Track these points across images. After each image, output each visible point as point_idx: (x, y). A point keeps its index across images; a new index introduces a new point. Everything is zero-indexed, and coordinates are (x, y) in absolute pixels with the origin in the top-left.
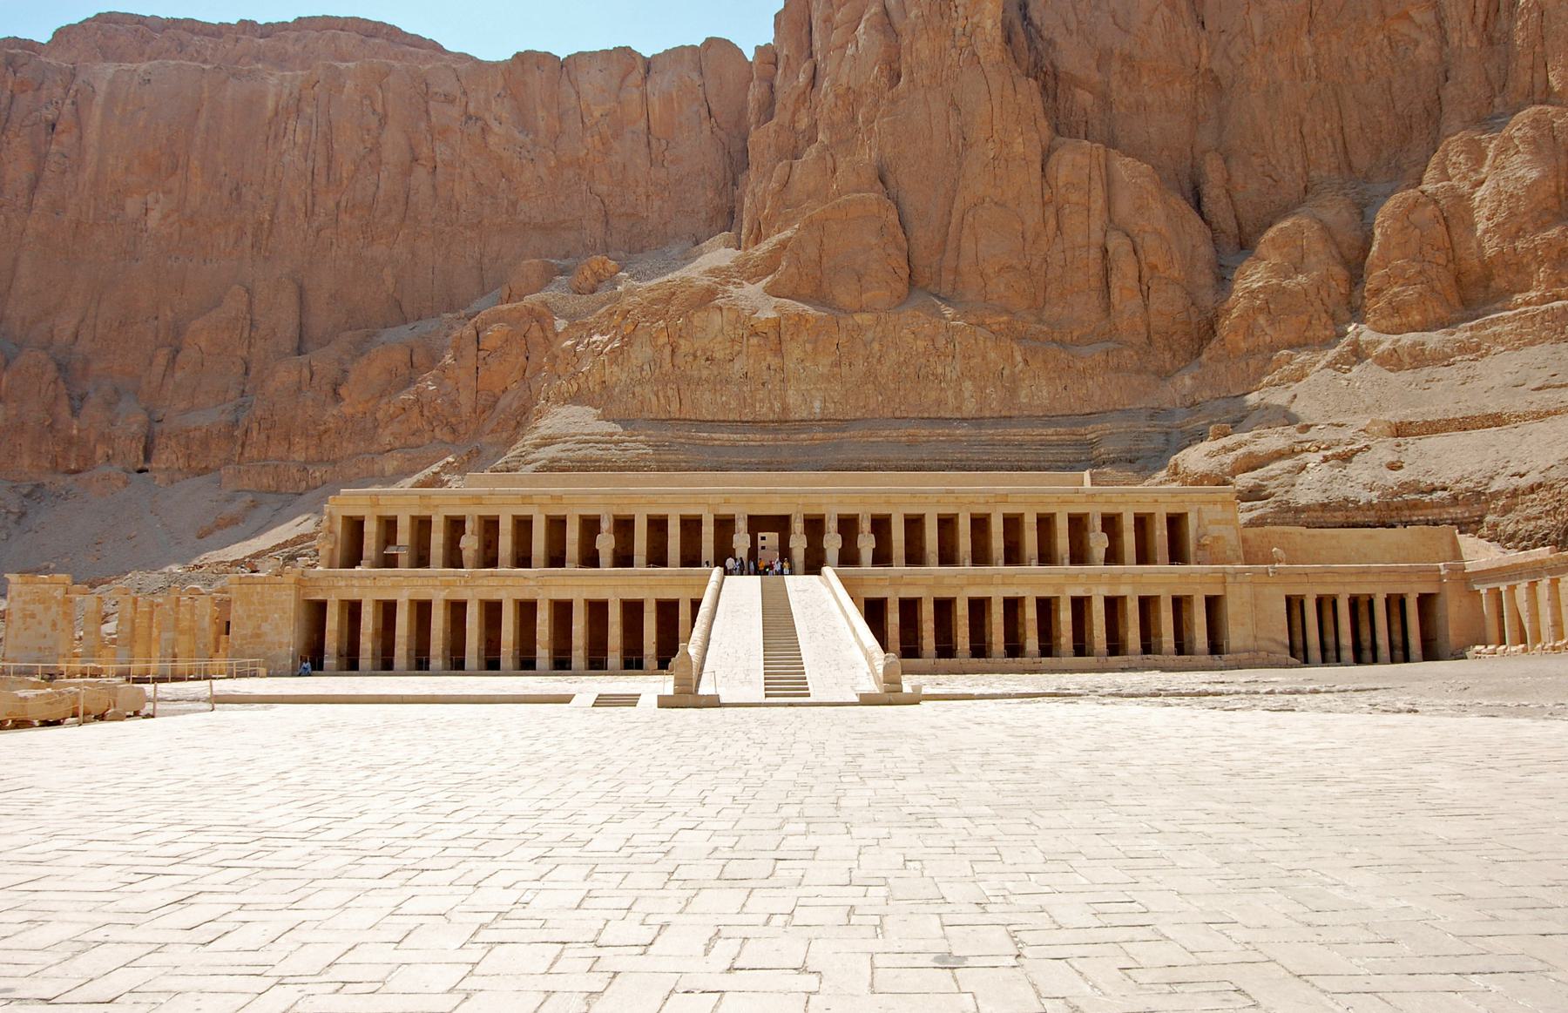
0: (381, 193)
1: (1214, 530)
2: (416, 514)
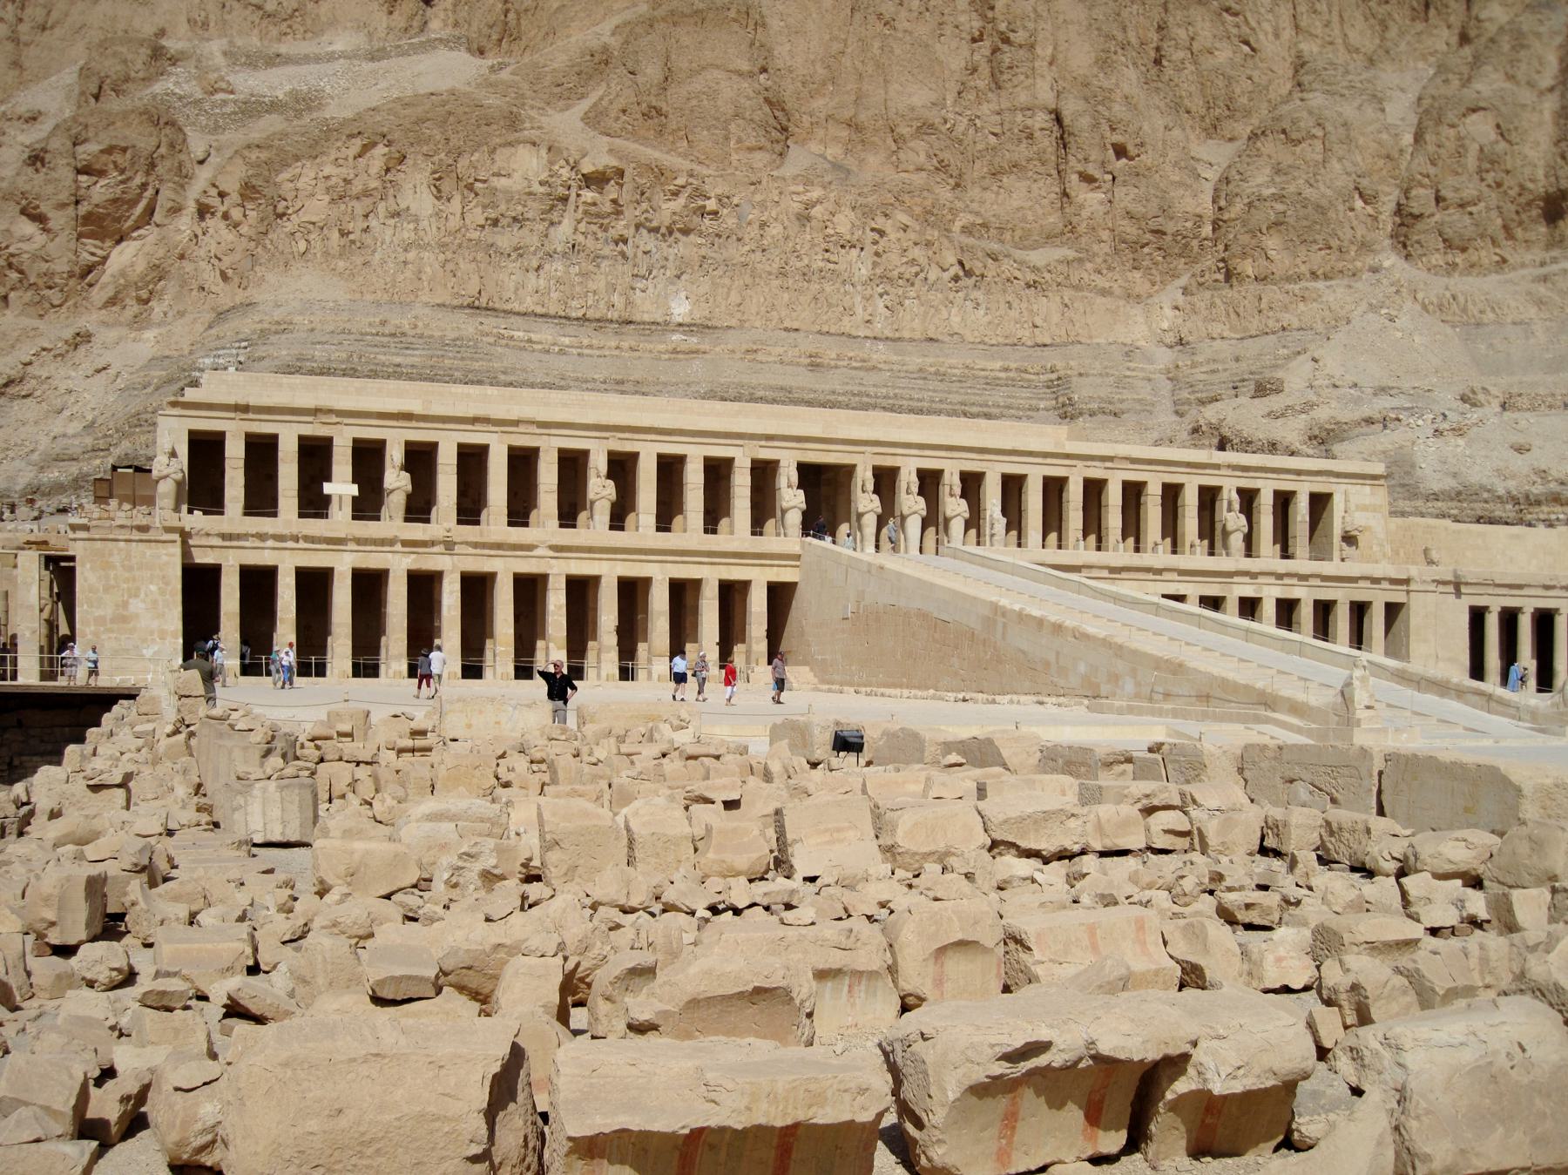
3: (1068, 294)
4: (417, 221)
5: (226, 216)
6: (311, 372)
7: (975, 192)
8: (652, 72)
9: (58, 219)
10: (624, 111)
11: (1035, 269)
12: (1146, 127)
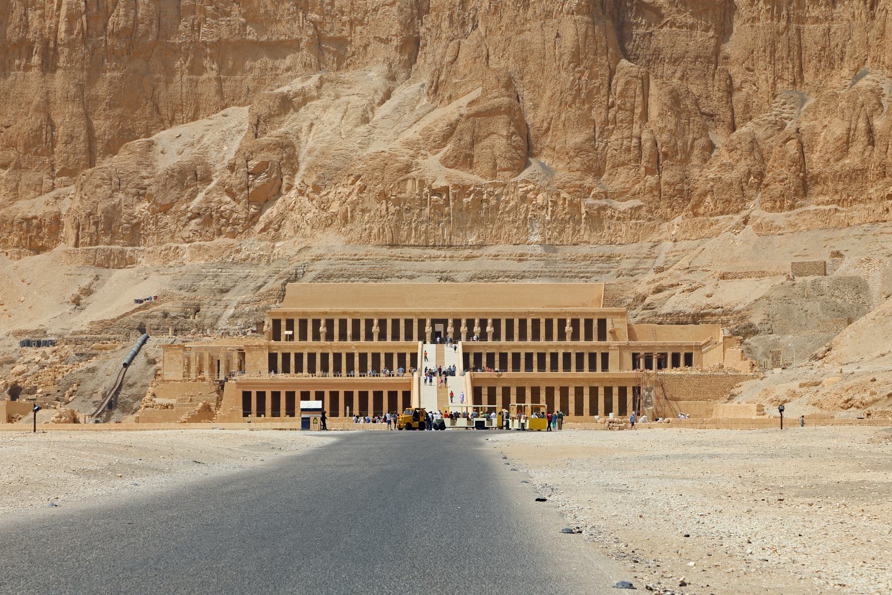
0: (139, 15)
1: (617, 326)
2: (301, 318)
3: (633, 221)
4: (370, 211)
5: (308, 196)
6: (329, 277)
7: (605, 176)
8: (467, 138)
9: (241, 196)
10: (455, 157)
11: (620, 212)
12: (679, 143)
